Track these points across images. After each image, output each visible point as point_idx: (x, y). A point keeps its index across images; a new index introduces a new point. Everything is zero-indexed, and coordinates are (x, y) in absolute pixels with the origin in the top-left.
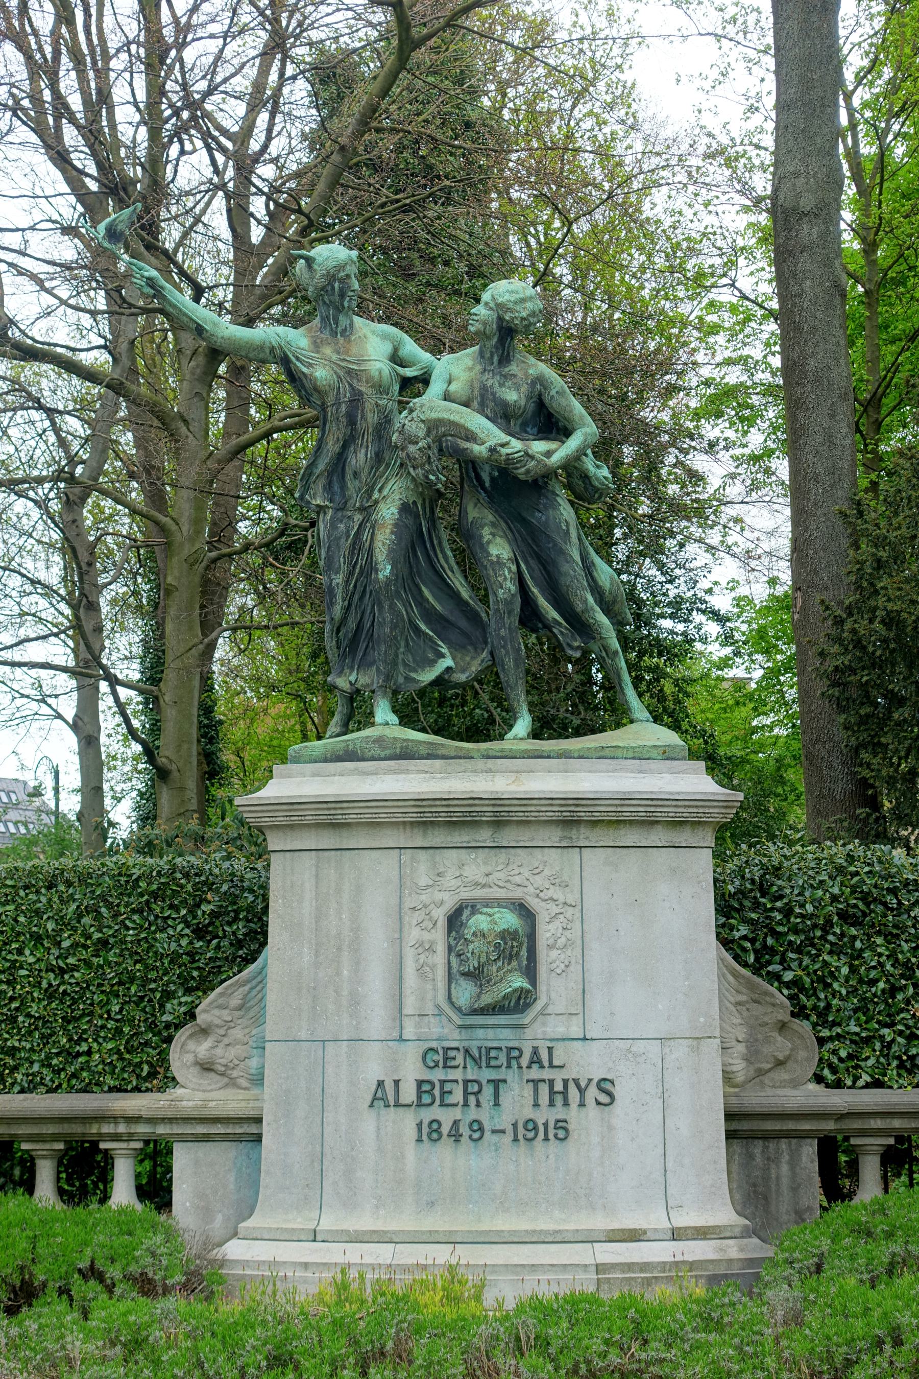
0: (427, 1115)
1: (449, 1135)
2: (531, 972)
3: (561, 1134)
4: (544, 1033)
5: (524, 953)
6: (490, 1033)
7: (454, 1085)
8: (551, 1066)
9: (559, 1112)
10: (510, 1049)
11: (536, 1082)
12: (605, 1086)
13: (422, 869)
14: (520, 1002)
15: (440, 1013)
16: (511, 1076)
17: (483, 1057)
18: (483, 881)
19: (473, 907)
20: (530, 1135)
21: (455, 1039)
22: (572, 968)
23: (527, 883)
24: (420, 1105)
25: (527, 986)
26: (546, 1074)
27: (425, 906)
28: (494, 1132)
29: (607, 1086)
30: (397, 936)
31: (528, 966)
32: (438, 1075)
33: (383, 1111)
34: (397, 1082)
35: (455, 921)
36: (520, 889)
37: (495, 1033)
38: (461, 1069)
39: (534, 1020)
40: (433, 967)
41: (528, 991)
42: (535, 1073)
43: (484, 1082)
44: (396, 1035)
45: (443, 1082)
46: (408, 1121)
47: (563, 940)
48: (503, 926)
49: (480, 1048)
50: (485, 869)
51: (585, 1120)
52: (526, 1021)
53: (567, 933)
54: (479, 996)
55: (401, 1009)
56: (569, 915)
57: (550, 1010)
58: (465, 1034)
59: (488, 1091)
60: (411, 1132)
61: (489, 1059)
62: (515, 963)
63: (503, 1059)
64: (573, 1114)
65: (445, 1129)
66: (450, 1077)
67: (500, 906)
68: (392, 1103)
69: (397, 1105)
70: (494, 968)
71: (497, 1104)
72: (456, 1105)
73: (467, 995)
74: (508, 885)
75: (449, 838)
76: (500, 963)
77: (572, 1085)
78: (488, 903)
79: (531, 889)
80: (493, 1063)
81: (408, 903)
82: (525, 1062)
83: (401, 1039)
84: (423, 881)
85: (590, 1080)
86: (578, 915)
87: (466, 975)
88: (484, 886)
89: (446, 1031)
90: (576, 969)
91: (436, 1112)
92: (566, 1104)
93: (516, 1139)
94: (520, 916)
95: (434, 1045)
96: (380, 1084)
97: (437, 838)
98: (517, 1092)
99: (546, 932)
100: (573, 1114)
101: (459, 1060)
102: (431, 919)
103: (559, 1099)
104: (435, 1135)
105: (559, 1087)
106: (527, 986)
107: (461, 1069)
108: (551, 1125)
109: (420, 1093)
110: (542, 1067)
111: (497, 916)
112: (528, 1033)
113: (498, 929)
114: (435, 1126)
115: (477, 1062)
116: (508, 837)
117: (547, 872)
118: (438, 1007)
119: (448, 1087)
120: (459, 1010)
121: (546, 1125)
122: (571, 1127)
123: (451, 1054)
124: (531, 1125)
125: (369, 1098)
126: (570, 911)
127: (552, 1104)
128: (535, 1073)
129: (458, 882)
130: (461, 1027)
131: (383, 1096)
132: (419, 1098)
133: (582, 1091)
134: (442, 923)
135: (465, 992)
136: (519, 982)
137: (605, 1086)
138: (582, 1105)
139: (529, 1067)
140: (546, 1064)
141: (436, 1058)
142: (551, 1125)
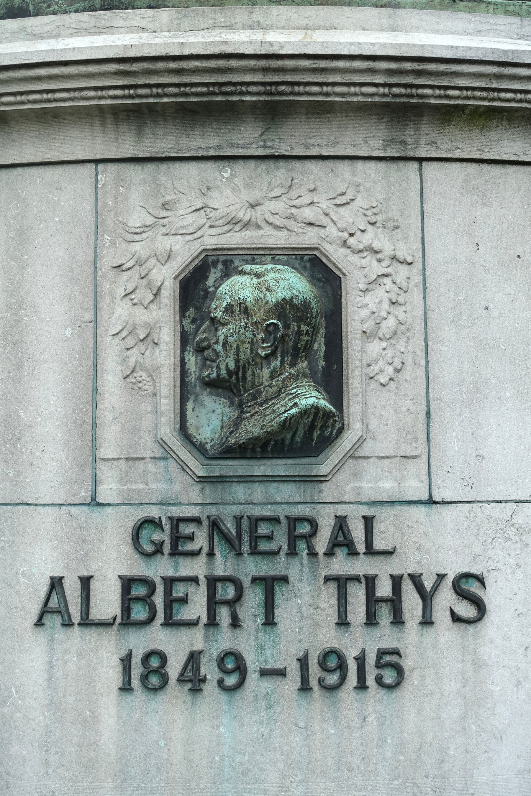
0: (140, 642)
1: (181, 680)
2: (332, 379)
3: (389, 677)
4: (357, 491)
5: (320, 346)
6: (258, 492)
7: (191, 589)
8: (370, 551)
9: (384, 637)
10: (294, 521)
11: (342, 583)
12: (469, 587)
13: (135, 194)
14: (313, 436)
15: (166, 454)
16: (297, 570)
17: (244, 536)
18: (245, 215)
19: (227, 263)
20: (332, 679)
21: (192, 501)
22: (406, 374)
23: (324, 220)
24: (127, 622)
25: (325, 404)
26: (361, 566)
27: (140, 263)
28: (264, 673)
29: (474, 587)
30: (89, 316)
31: (327, 370)
32: (161, 568)
33: (61, 634)
34: (86, 582)
35: (194, 288)
36: (312, 232)
37: (267, 492)
38: (203, 558)
39: (338, 467)
40: (153, 373)
41: (328, 415)
42: (341, 565)
43: (246, 582)
44: (85, 495)
45: (170, 582)
46: (104, 654)
47: (391, 322)
48: (281, 293)
49: (238, 520)
50: (247, 196)
51: (432, 650)
52: (324, 469)
53: (398, 311)
54: (237, 424)
55: (94, 447)
56: (401, 278)
57: (366, 450)
58: (211, 493)
59: (254, 598)
60: (112, 674)
61: (255, 539)
62: (303, 365)
63: (281, 540)
64: (411, 640)
65: (174, 669)
66: (184, 572)
67: (274, 261)
68: (76, 618)
69: (86, 622)
70: (266, 372)
71: (270, 621)
72: (192, 624)
73: (215, 422)
74: (291, 224)
75: (184, 142)
76: (276, 363)
77: (408, 587)
78: (255, 255)
79: (332, 231)
80: (263, 546)
81: (110, 258)
82: (321, 544)
83: (94, 503)
84: (137, 218)
85: (441, 577)
86: (417, 279)
87: (214, 385)
88: (247, 225)
89: (177, 487)
90: (413, 375)
91: (158, 637)
92: (398, 620)
93: (305, 687)
94: (313, 279)
95: (154, 512)
96: (56, 584)
97: (162, 141)
98: (307, 598)
99: (360, 309)
100: (411, 640)
101: (201, 541)
102: (149, 286)
103: (385, 614)
104: (154, 680)
105: (384, 589)
106: (325, 404)
107: (203, 558)
108: (371, 659)
109: (127, 601)
110: (353, 553)
111: (271, 277)
112: (328, 492)
113: (272, 299)
114: (155, 663)
115: (233, 545)
116: (293, 137)
117: (360, 202)
118: (162, 444)
119: (179, 590)
120: (199, 448)
121: (361, 660)
122: (407, 663)
123: (186, 529)
124: (333, 661)
125: (35, 609)
126: (403, 272)
127: (371, 620)
128: (341, 565)
129: (201, 218)
130: (203, 480)
131: (60, 606)
132: (126, 610)
133: (426, 597)
134: (170, 292)
135: (211, 418)
136: (310, 397)
137: (469, 587)
138: (427, 621)
139: (330, 554)
140: (361, 547)
141: (157, 536)
142: (371, 659)
